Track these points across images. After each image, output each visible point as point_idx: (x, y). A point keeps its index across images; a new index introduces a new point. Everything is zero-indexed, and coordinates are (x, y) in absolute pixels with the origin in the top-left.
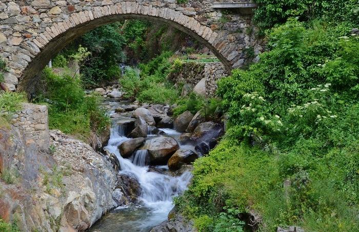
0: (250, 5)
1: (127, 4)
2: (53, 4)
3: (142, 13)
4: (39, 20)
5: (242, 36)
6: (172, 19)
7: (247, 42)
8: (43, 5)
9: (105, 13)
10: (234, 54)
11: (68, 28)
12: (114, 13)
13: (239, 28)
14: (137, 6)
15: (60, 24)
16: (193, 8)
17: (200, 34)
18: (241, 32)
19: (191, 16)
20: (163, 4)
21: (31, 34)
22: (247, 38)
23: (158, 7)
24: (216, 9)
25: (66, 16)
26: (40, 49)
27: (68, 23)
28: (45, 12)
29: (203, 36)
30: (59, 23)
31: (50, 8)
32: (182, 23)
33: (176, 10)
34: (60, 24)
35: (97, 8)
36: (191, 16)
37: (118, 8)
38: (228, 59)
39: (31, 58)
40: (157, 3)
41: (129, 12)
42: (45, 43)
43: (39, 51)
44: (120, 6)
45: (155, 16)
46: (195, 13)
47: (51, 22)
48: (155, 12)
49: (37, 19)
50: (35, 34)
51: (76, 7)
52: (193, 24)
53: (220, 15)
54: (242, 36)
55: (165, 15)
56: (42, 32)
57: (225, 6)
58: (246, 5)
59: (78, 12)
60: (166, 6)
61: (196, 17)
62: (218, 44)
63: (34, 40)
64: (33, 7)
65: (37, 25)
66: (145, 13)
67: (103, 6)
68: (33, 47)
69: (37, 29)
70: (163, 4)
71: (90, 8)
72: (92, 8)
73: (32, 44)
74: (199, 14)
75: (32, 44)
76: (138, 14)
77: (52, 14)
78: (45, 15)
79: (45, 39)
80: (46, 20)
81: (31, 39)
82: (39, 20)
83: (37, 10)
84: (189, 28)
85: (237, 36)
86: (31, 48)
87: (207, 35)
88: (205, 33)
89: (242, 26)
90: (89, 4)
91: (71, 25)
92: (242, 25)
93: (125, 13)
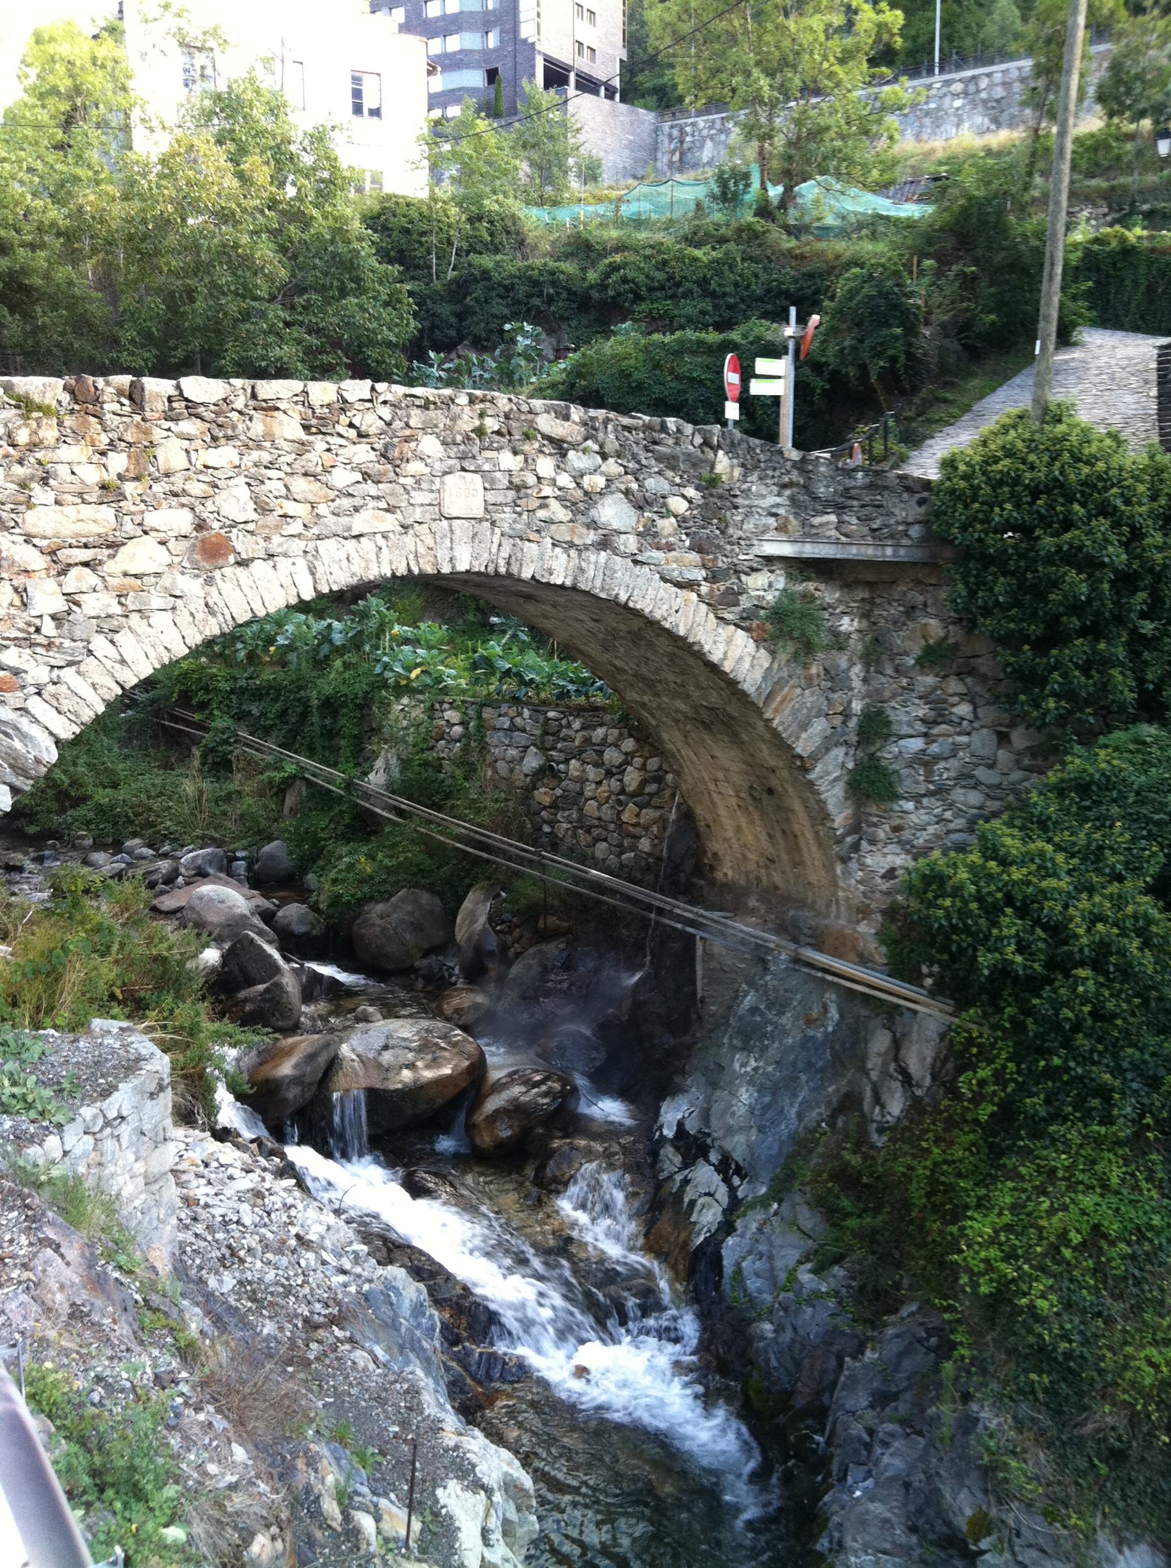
0: (902, 552)
1: (458, 532)
2: (129, 527)
3: (514, 569)
4: (60, 605)
5: (843, 661)
6: (623, 597)
7: (857, 684)
8: (81, 528)
9: (367, 568)
10: (819, 726)
11: (199, 639)
12: (402, 571)
13: (836, 634)
14: (496, 540)
15: (161, 620)
16: (694, 557)
17: (715, 657)
18: (841, 649)
19: (689, 585)
20: (591, 537)
21: (16, 672)
22: (857, 670)
23: (571, 545)
24: (769, 560)
25: (191, 586)
26: (58, 742)
27: (200, 616)
28: (86, 564)
29: (727, 667)
30: (156, 618)
31: (114, 546)
32: (657, 615)
33: (636, 562)
34: (161, 620)
35: (332, 542)
36: (689, 585)
37: (422, 550)
38: (799, 750)
39: (15, 790)
40: (572, 531)
41: (462, 566)
42: (87, 716)
43: (52, 755)
44: (429, 541)
45: (562, 587)
46: (699, 574)
47: (117, 610)
48: (560, 569)
49: (47, 598)
50: (38, 673)
51: (242, 544)
52: (688, 616)
53: (781, 582)
54: (843, 661)
55: (598, 583)
56: (70, 664)
57: (810, 550)
58: (889, 551)
59: (242, 563)
60: (604, 544)
61: (705, 589)
62: (770, 696)
63: (36, 705)
64: (28, 539)
65: (49, 628)
66: (526, 574)
67: (357, 537)
68: (24, 737)
69: (49, 646)
70: (591, 537)
71: (298, 546)
72: (311, 546)
73: (24, 723)
74: (713, 578)
75: (24, 723)
76: (497, 574)
77: (125, 575)
78: (89, 578)
79: (89, 692)
80: (93, 605)
81: (14, 698)
82: (60, 605)
83: (53, 553)
84: (682, 632)
85: (828, 664)
86: (17, 744)
87: (741, 658)
88: (734, 653)
89: (846, 624)
90: (296, 527)
91: (213, 628)
92: (846, 620)
93: (446, 569)
